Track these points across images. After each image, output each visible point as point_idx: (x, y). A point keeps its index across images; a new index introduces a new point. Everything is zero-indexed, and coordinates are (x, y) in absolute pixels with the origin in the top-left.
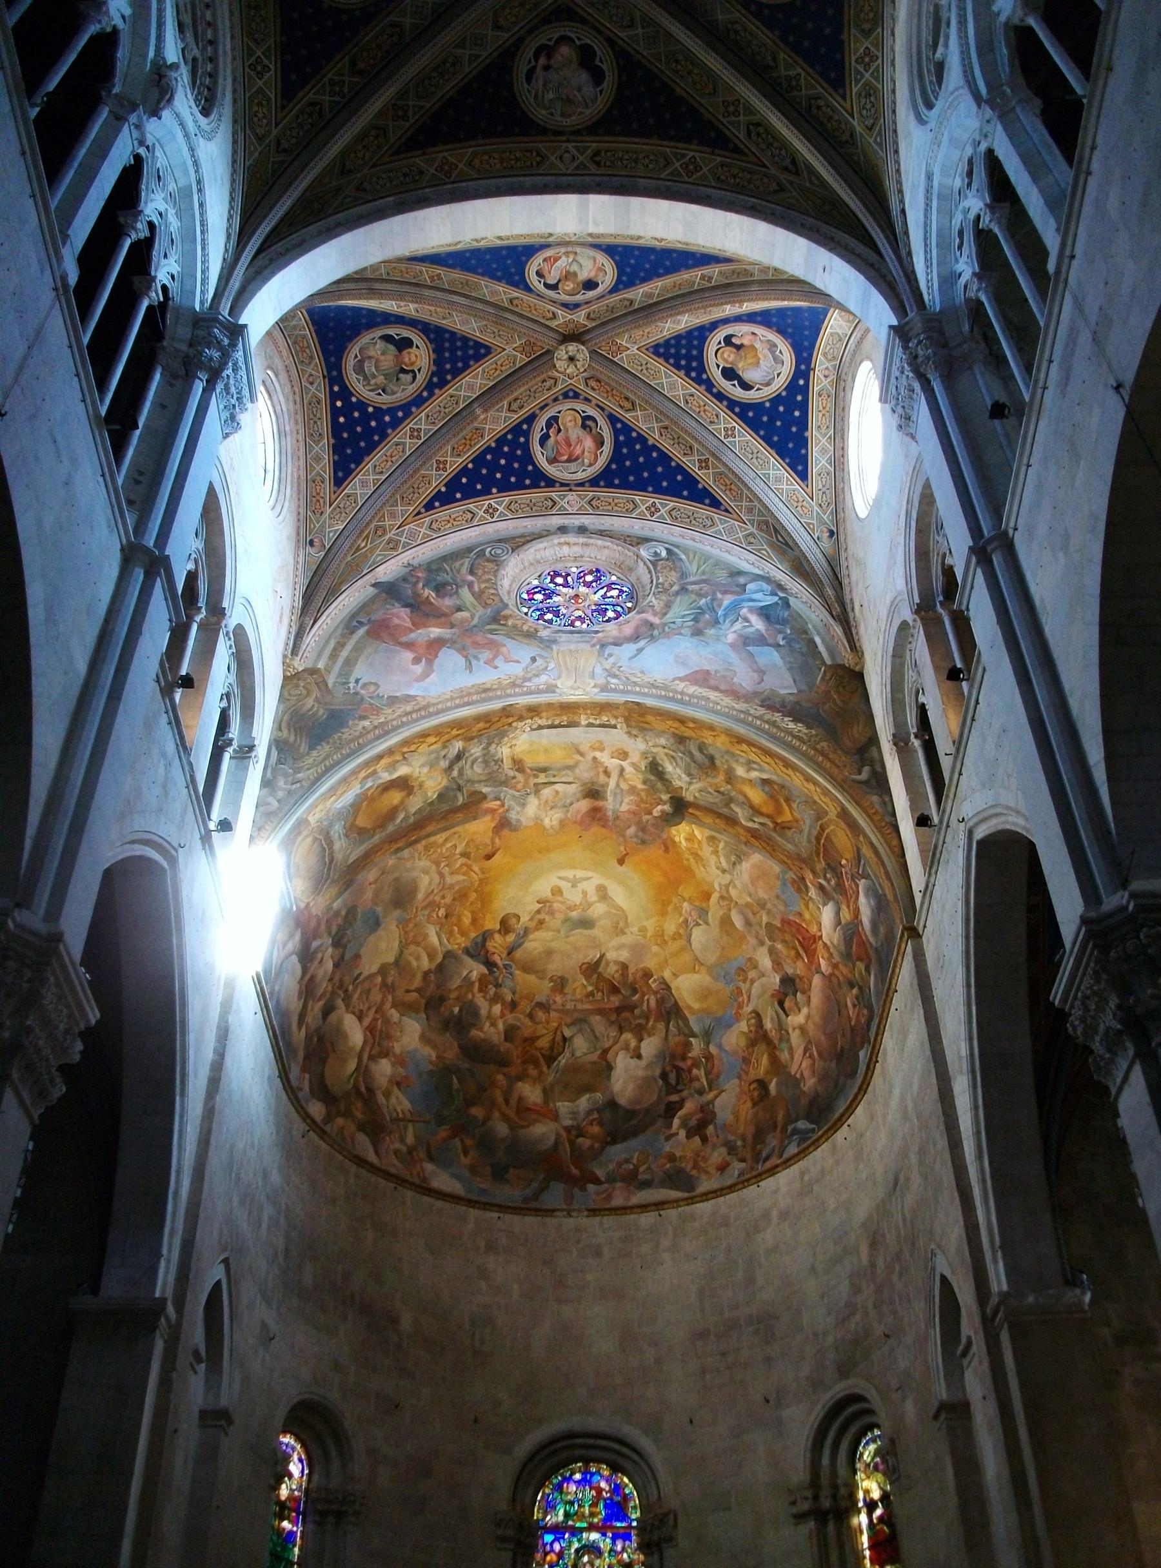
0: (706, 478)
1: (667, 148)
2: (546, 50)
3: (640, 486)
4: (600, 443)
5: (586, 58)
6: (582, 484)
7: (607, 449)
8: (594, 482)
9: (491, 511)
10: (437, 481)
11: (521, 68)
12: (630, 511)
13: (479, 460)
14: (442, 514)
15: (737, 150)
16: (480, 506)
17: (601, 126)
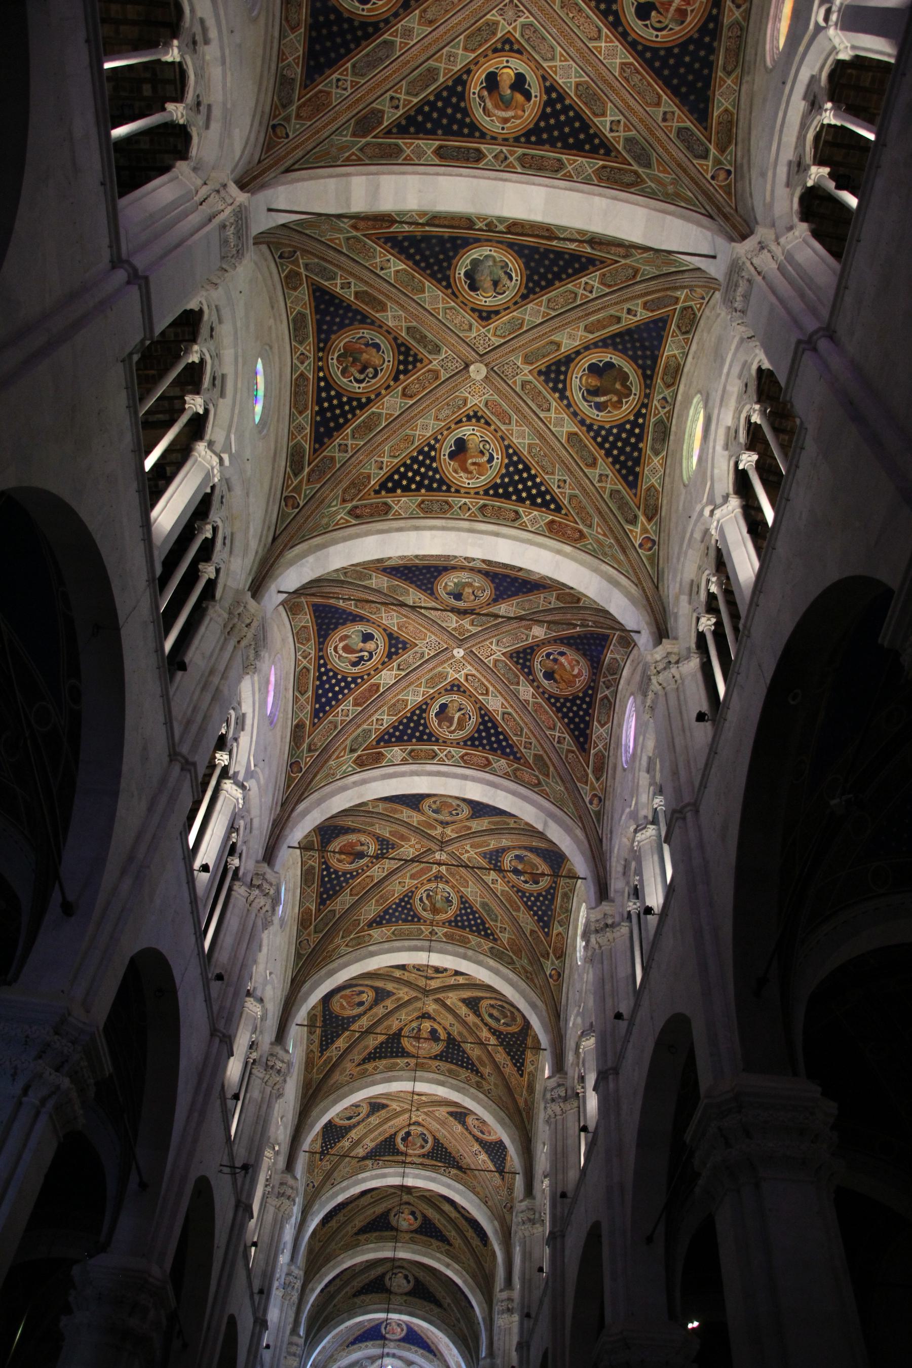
0: (433, 1347)
1: (426, 1303)
2: (396, 1274)
3: (413, 1344)
4: (402, 1330)
5: (406, 1277)
6: (396, 1340)
7: (405, 1332)
8: (400, 1340)
9: (367, 1346)
10: (351, 1339)
11: (387, 1277)
12: (409, 1350)
13: (365, 1332)
14: (351, 1348)
15: (445, 1309)
16: (363, 1345)
17: (408, 1294)
